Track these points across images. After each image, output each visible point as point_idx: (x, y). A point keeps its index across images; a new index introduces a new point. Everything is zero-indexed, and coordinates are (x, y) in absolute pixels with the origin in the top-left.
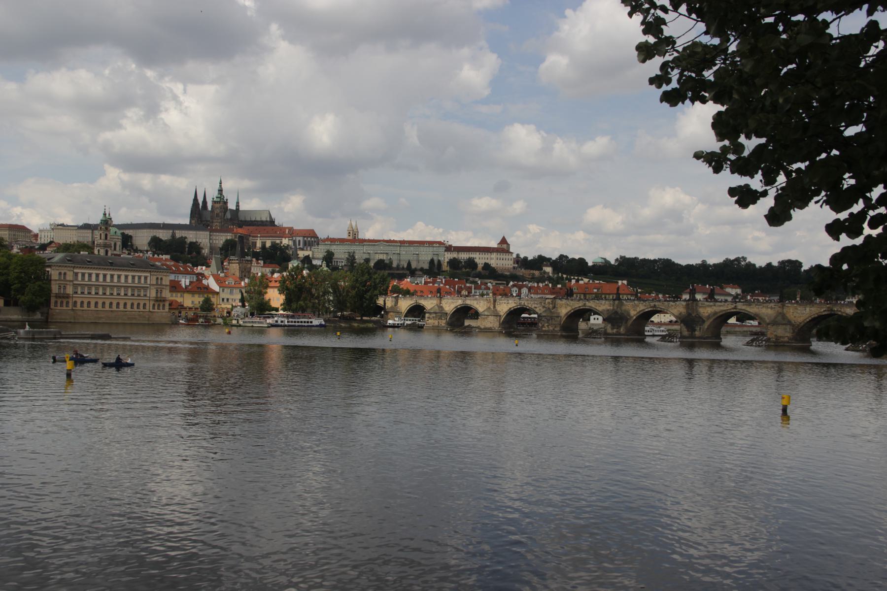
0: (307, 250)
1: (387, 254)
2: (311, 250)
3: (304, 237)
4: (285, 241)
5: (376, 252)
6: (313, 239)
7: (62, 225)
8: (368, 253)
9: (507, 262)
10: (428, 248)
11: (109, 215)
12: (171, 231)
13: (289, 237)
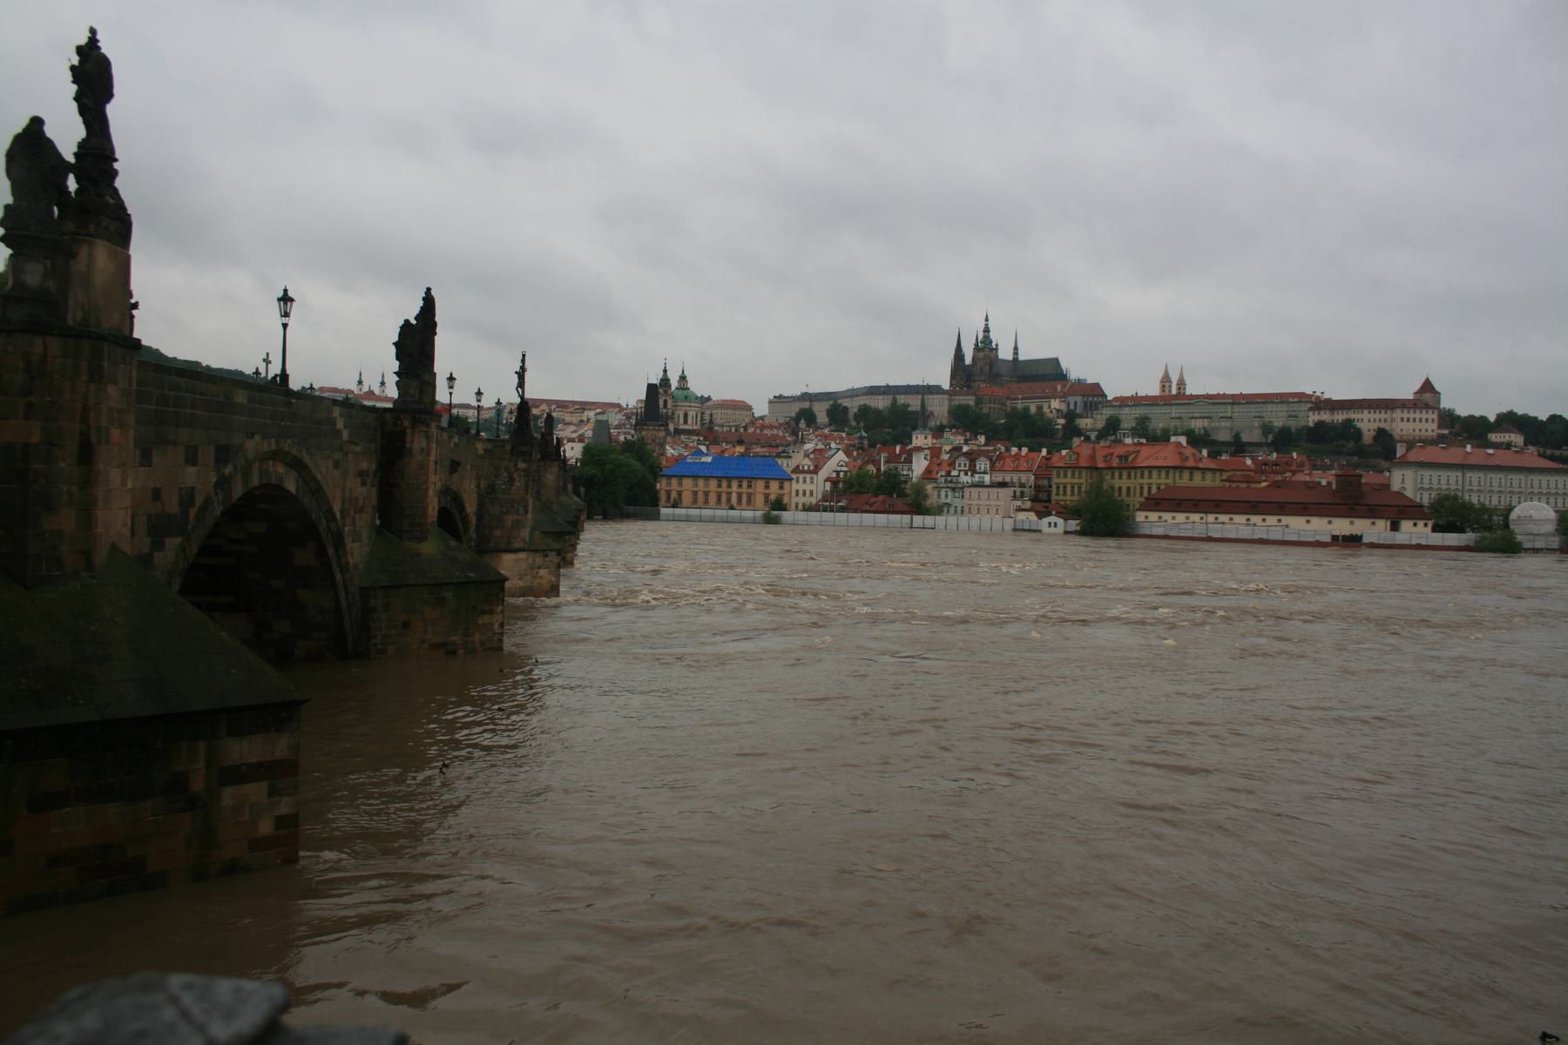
0: (1087, 417)
1: (1210, 418)
2: (1092, 417)
3: (1084, 396)
4: (1055, 404)
5: (1191, 415)
6: (1095, 399)
7: (780, 397)
8: (1180, 418)
9: (1424, 426)
10: (1279, 406)
11: (683, 371)
12: (891, 397)
13: (1061, 398)
